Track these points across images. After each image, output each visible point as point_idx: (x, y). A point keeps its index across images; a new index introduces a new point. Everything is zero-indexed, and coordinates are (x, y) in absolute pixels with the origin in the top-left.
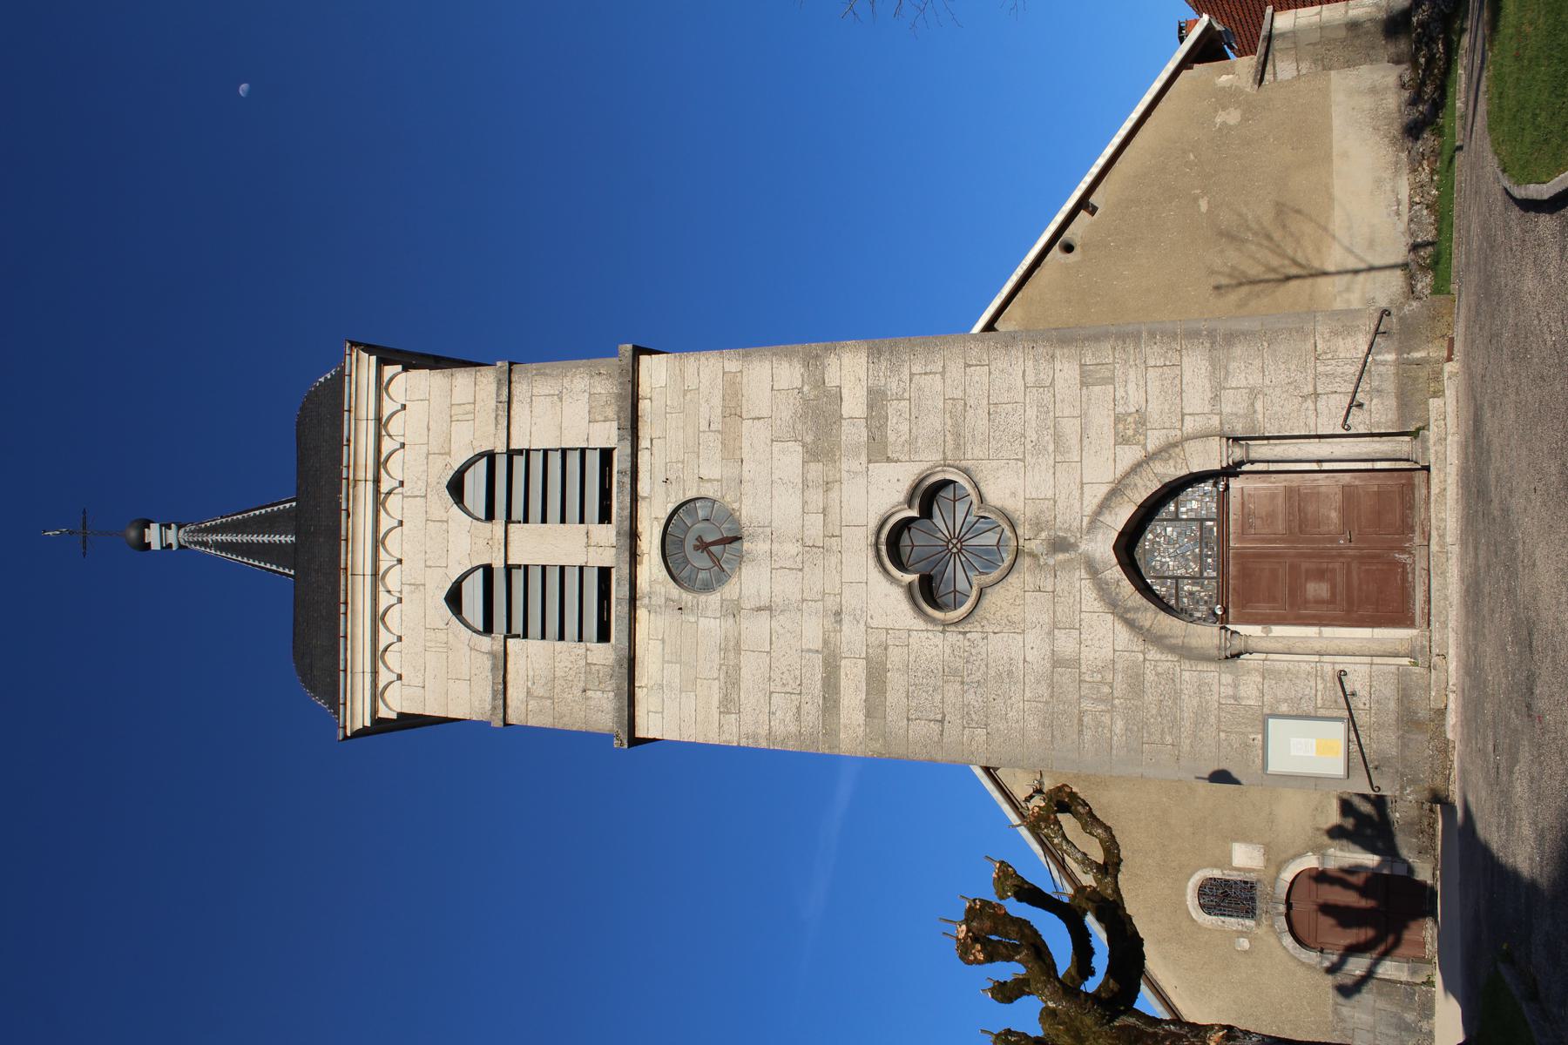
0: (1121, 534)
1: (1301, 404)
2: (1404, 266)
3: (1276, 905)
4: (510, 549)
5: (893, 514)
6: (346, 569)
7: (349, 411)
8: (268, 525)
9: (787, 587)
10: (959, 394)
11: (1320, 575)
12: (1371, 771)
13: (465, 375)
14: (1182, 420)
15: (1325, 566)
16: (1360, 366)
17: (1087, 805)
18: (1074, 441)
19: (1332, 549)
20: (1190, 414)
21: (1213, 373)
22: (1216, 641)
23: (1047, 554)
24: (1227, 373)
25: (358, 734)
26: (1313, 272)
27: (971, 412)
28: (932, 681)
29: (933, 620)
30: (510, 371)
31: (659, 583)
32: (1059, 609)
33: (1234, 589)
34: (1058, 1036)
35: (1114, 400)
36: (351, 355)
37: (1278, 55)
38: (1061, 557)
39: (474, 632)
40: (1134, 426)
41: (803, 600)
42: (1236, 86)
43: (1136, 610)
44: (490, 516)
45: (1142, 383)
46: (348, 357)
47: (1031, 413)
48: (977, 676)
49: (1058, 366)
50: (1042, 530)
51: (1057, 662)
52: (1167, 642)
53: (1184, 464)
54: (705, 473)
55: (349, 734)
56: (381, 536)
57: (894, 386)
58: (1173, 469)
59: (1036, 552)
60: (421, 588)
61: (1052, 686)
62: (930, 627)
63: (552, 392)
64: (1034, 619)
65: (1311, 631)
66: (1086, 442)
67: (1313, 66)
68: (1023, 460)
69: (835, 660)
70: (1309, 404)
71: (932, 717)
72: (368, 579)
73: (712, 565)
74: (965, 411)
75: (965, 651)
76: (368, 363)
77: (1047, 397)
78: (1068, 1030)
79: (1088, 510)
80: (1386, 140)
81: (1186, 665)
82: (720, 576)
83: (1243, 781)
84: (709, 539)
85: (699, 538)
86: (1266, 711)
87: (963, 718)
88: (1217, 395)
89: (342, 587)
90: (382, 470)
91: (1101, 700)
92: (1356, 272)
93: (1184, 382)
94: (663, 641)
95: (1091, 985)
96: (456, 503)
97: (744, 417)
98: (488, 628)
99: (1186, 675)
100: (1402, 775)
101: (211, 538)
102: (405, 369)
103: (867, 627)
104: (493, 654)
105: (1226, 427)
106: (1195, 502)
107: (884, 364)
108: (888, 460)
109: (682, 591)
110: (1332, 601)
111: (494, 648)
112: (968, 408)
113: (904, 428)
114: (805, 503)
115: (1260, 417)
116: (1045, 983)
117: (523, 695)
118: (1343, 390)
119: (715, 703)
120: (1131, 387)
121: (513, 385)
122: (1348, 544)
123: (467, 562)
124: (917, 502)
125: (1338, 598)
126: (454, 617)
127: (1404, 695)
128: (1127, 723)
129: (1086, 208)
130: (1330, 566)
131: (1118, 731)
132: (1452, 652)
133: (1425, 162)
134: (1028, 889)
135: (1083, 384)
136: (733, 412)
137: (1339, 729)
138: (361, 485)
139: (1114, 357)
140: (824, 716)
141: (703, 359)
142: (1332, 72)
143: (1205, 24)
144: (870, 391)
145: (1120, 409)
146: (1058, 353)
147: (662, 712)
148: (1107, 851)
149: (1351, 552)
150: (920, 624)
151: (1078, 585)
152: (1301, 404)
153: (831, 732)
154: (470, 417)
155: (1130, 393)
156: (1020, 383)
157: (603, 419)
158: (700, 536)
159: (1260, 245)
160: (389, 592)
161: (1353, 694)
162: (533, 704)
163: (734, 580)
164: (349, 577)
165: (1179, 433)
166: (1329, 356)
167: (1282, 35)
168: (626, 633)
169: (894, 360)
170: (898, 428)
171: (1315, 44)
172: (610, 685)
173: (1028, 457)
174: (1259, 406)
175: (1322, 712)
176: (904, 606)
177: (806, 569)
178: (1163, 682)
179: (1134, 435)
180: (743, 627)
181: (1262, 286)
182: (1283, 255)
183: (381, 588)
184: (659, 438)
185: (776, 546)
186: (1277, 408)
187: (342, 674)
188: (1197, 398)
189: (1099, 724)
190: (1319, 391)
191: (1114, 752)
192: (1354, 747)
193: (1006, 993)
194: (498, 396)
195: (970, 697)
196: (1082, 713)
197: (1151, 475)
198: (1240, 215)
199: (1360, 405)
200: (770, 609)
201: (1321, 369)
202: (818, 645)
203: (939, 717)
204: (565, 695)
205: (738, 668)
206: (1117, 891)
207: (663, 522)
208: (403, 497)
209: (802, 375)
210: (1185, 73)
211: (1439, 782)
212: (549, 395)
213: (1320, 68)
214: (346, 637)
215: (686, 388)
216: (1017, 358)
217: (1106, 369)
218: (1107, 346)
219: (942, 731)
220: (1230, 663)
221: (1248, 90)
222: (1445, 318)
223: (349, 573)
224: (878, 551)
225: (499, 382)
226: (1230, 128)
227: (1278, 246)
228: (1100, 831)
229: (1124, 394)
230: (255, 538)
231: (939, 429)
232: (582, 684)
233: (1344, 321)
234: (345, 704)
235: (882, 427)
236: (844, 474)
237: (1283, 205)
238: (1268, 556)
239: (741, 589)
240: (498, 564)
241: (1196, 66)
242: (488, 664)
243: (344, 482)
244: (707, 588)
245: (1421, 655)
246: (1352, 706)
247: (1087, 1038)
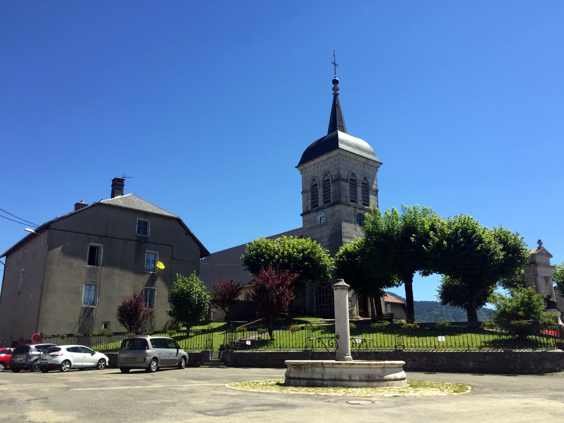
117: (343, 184)
119: (346, 219)
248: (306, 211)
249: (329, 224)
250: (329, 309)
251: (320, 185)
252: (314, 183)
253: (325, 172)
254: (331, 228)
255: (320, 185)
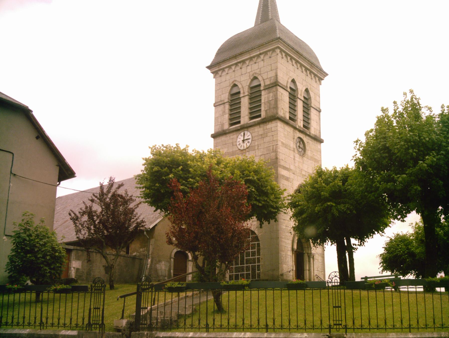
248: (220, 130)
249: (256, 148)
250: (251, 272)
251: (244, 93)
252: (235, 90)
253: (253, 75)
254: (260, 154)
255: (244, 93)
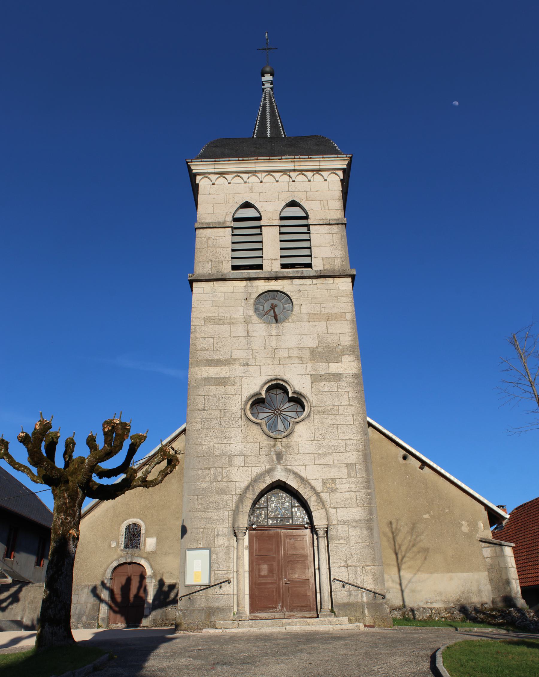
0: (285, 483)
1: (343, 560)
2: (404, 606)
3: (130, 558)
4: (269, 227)
5: (290, 386)
6: (257, 160)
7: (323, 158)
8: (274, 125)
9: (258, 343)
10: (341, 412)
11: (271, 571)
12: (188, 596)
13: (340, 205)
14: (334, 508)
15: (275, 573)
16: (360, 586)
17: (171, 472)
18: (323, 461)
19: (282, 575)
20: (337, 511)
21: (354, 521)
22: (241, 526)
23: (275, 451)
24: (355, 527)
25: (189, 168)
26: (400, 565)
27: (333, 417)
28: (220, 405)
29: (246, 404)
30: (342, 224)
31: (257, 290)
32: (253, 457)
33: (263, 533)
34: (73, 465)
35: (341, 478)
36: (346, 157)
37: (493, 549)
38: (274, 457)
39: (234, 214)
40: (331, 487)
41: (252, 350)
42: (478, 531)
43: (253, 491)
44: (282, 218)
45: (349, 490)
46: (345, 156)
47: (334, 443)
48: (223, 424)
49: (355, 454)
50: (285, 449)
51: (230, 457)
52: (240, 505)
53: (315, 509)
54: (304, 307)
55: (189, 164)
56: (272, 173)
57: (343, 384)
58: (313, 504)
59: (276, 446)
60: (251, 191)
61: (220, 455)
62: (243, 403)
63: (334, 242)
64: (248, 447)
65: (247, 568)
66: (323, 466)
67: (489, 564)
68: (314, 440)
69: (228, 364)
70: (343, 564)
71: (206, 405)
72: (253, 169)
73: (265, 311)
74: (334, 415)
75: (234, 418)
76: (343, 164)
77: (341, 449)
78: (75, 469)
79: (295, 469)
80: (458, 597)
81: (231, 513)
82: (261, 315)
83: (182, 540)
84: (276, 309)
85: (276, 306)
86: (212, 549)
87: (206, 418)
88: (345, 523)
89: (250, 158)
90: (299, 173)
91: (215, 477)
92: (401, 584)
93: (350, 508)
94: (233, 292)
95: (95, 478)
96: (286, 204)
97: (328, 322)
98: (235, 220)
99: (226, 513)
100: (187, 610)
101: (267, 102)
102: (341, 180)
103: (242, 377)
104: (225, 222)
105: (332, 527)
106: (299, 515)
107: (352, 380)
108: (312, 383)
109: (254, 299)
110: (260, 576)
111: (227, 223)
112: (335, 416)
113: (326, 389)
114: (293, 349)
115: (337, 542)
116: (95, 458)
117: (208, 235)
118: (350, 579)
120: (347, 485)
121: (337, 225)
122: (284, 583)
123: (262, 210)
124: (295, 395)
125: (261, 579)
126: (239, 205)
127: (221, 610)
128: (206, 488)
129: (422, 465)
130: (275, 575)
131: (202, 485)
132: (240, 630)
133: (449, 615)
134: (135, 448)
135: (348, 465)
136: (330, 317)
137: (206, 582)
138: (292, 164)
139: (359, 478)
140: (205, 360)
141: (351, 304)
142: (487, 573)
143: (505, 516)
144: (340, 374)
145: (337, 481)
146: (360, 453)
147: (204, 293)
148: (152, 481)
149: (281, 584)
150: (244, 399)
151: (263, 465)
152: (343, 560)
153: (198, 363)
154: (323, 208)
155: (344, 485)
156: (347, 438)
157: (324, 263)
158: (277, 306)
159: (410, 542)
160: (249, 178)
161: (221, 587)
162: (205, 239)
163: (260, 321)
164: (254, 161)
165: (328, 507)
166: (364, 572)
167: (502, 551)
168: (236, 277)
169: (354, 384)
170: (325, 386)
171: (499, 565)
172: (214, 271)
173: (316, 442)
174: (342, 541)
175: (212, 573)
176: (252, 392)
177: (265, 350)
178: (223, 503)
179: (327, 487)
180: (240, 325)
181: (392, 542)
182: (406, 552)
183: (250, 175)
184: (317, 287)
185: (274, 337)
186: (341, 549)
187: (214, 160)
188: (344, 514)
189: (205, 476)
190: (349, 568)
191: (193, 483)
192: (198, 588)
193: (91, 442)
194: (332, 219)
195: (215, 421)
196: (209, 469)
197: (310, 495)
198: (423, 533)
199: (344, 586)
200: (248, 336)
201: (358, 568)
202: (234, 357)
203: (206, 409)
204: (209, 253)
205: (223, 324)
206: (135, 487)
207: (282, 290)
208: (288, 182)
209: (346, 346)
210: (483, 508)
211: (184, 626)
212: (333, 241)
213: (488, 567)
214: (229, 161)
215: (339, 297)
216: (357, 436)
217: (354, 475)
218: (364, 474)
219: (200, 410)
220: (232, 532)
221: (477, 535)
222: (383, 624)
223: (256, 161)
224: (274, 380)
225: (338, 220)
226: (460, 528)
227: (410, 549)
228: (160, 478)
229: (344, 482)
230: (268, 120)
231: (326, 404)
232: (214, 260)
233: (379, 579)
234: (201, 162)
235: (326, 380)
236: (305, 365)
237: (428, 552)
238: (278, 547)
239: (256, 324)
240: (262, 223)
241: (486, 512)
242: (220, 220)
243: (293, 157)
244: (256, 310)
245: (238, 617)
246: (215, 587)
247: (72, 477)
